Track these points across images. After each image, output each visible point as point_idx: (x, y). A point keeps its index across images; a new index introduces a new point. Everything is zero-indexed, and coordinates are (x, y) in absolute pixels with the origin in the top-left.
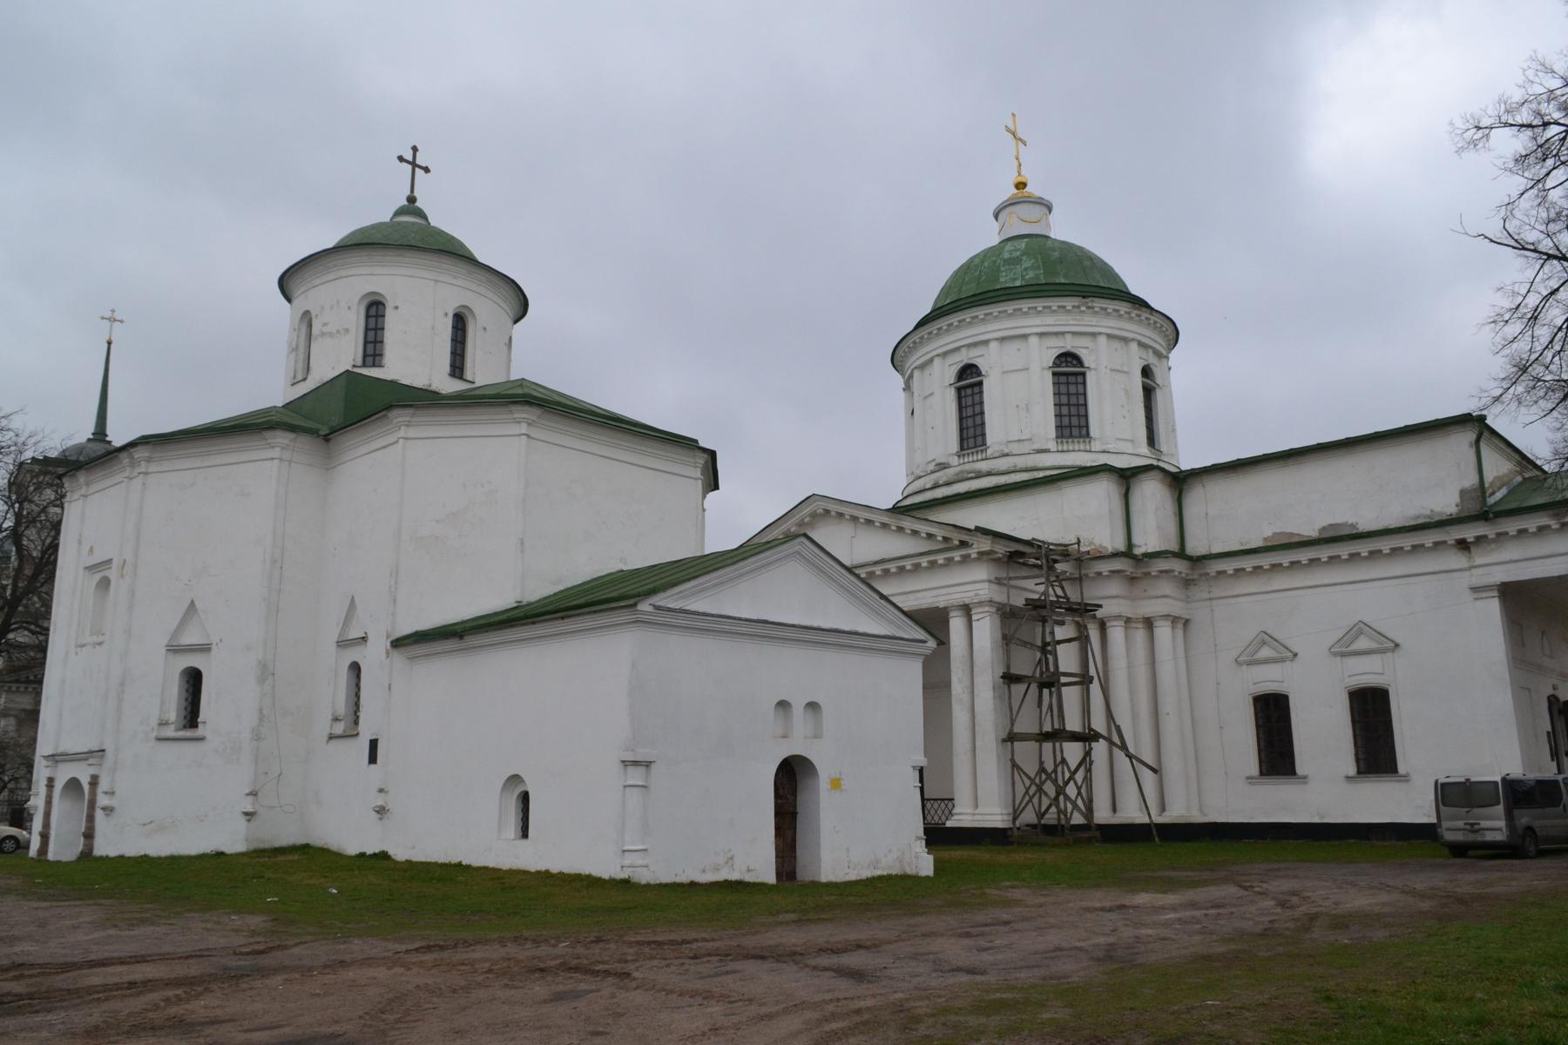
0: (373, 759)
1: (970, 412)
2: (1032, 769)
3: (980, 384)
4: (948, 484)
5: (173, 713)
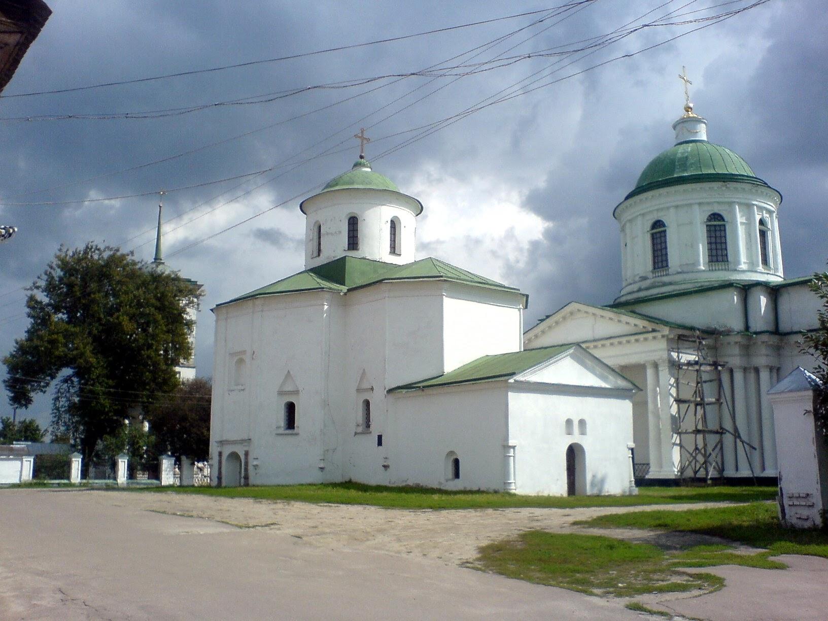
0: (380, 443)
1: (659, 247)
2: (691, 449)
3: (665, 231)
4: (647, 289)
5: (282, 422)
